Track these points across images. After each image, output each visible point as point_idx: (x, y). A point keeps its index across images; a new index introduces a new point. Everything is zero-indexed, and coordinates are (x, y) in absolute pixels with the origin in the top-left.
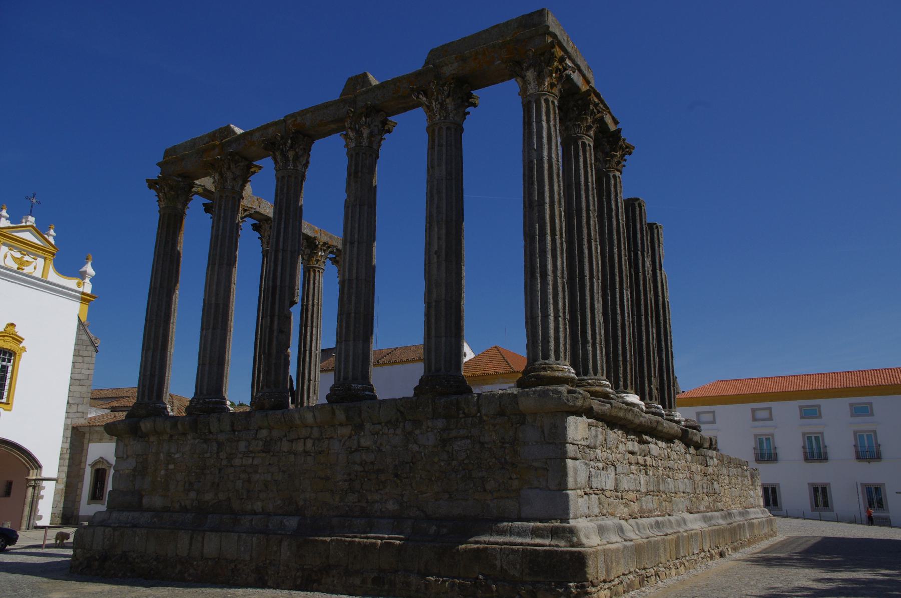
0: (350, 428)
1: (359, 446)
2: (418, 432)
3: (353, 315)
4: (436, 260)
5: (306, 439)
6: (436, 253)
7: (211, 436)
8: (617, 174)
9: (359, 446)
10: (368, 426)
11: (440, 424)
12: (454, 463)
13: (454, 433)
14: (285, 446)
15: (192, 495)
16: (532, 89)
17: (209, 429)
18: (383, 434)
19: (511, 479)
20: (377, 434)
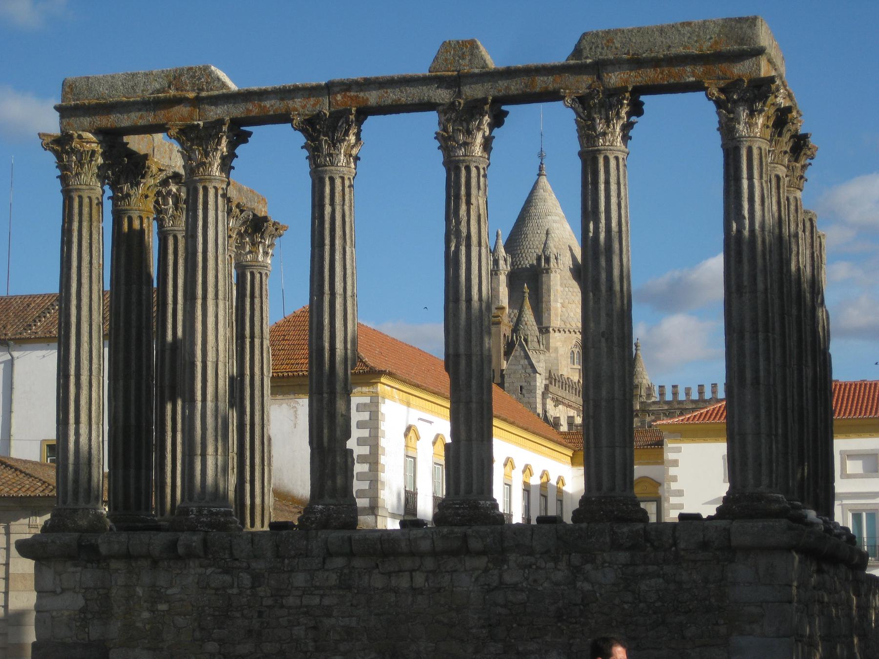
0: (484, 560)
1: (501, 583)
2: (588, 567)
3: (474, 406)
4: (603, 344)
5: (412, 571)
6: (603, 334)
7: (237, 564)
8: (799, 194)
9: (501, 583)
10: (512, 557)
11: (623, 557)
12: (642, 605)
13: (640, 569)
14: (378, 581)
15: (211, 647)
16: (742, 129)
17: (231, 554)
18: (538, 568)
19: (717, 624)
20: (530, 566)
